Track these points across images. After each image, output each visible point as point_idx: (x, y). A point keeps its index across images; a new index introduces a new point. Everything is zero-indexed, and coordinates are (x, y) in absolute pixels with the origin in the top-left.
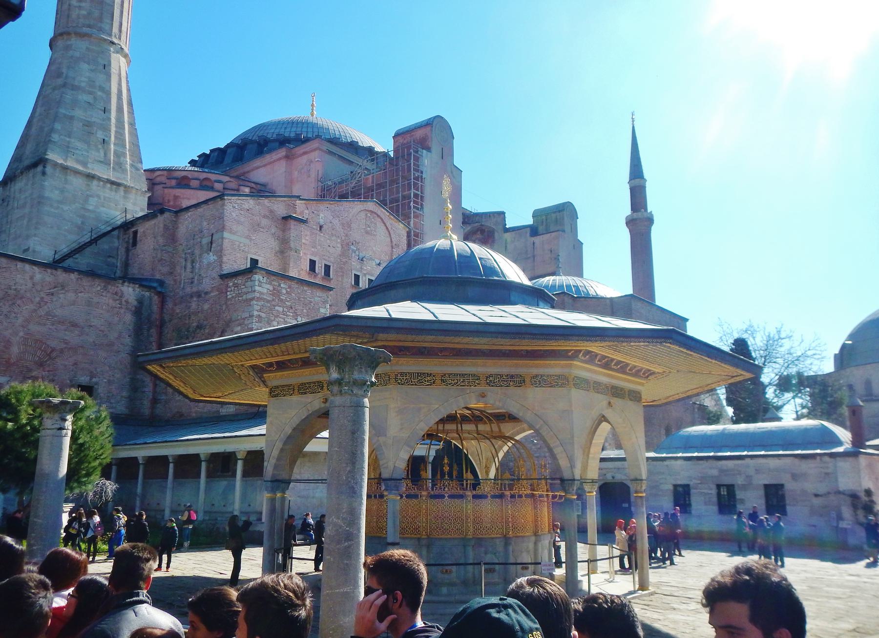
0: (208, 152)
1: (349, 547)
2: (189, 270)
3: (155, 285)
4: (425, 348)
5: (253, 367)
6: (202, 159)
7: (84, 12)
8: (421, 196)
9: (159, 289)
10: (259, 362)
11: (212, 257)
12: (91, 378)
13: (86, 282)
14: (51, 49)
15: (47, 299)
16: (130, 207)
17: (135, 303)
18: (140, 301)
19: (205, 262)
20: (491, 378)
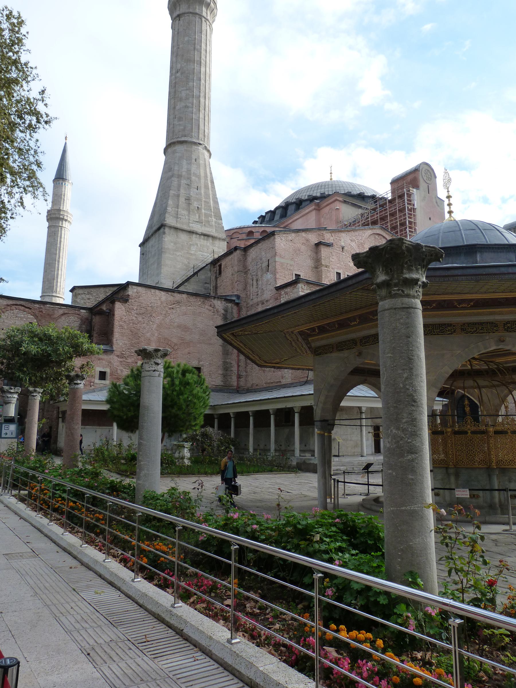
0: (264, 214)
1: (413, 460)
2: (255, 286)
3: (234, 298)
4: (445, 301)
5: (301, 333)
6: (261, 219)
7: (183, 128)
8: (414, 223)
9: (237, 301)
10: (304, 328)
11: (269, 276)
12: (199, 362)
13: (192, 299)
14: (165, 155)
15: (169, 311)
16: (216, 249)
17: (223, 312)
18: (226, 310)
19: (265, 279)
20: (509, 325)
